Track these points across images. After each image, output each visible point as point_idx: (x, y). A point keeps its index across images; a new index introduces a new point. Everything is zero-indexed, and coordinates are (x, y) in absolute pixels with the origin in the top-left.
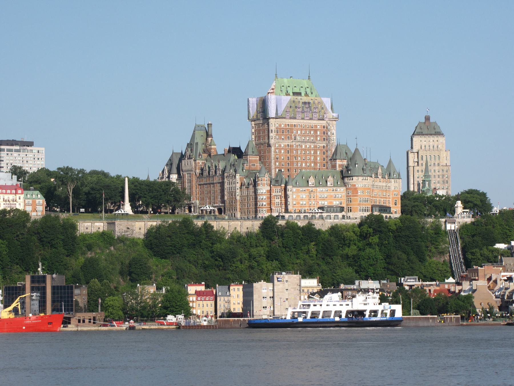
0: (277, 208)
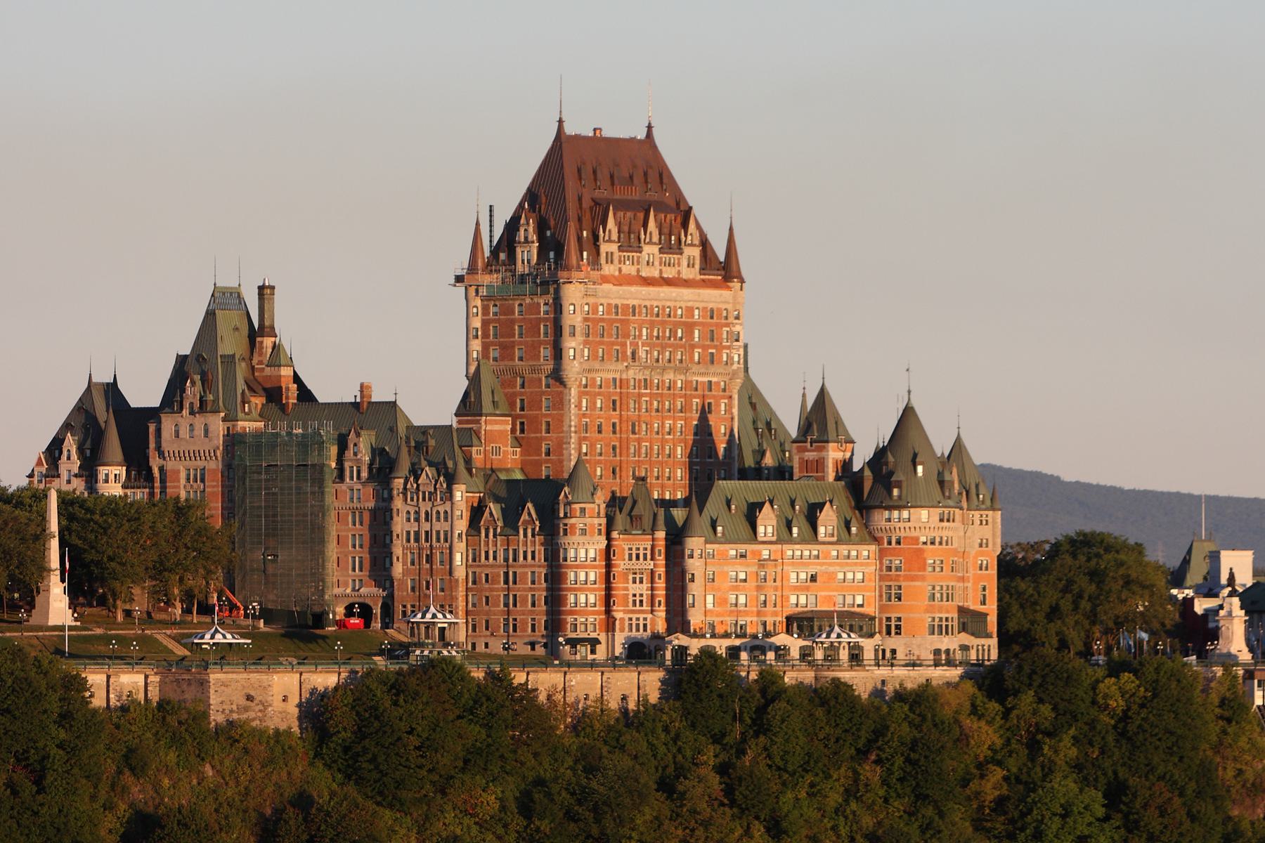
0: (634, 616)
